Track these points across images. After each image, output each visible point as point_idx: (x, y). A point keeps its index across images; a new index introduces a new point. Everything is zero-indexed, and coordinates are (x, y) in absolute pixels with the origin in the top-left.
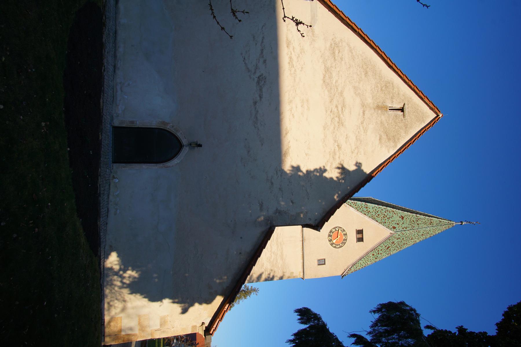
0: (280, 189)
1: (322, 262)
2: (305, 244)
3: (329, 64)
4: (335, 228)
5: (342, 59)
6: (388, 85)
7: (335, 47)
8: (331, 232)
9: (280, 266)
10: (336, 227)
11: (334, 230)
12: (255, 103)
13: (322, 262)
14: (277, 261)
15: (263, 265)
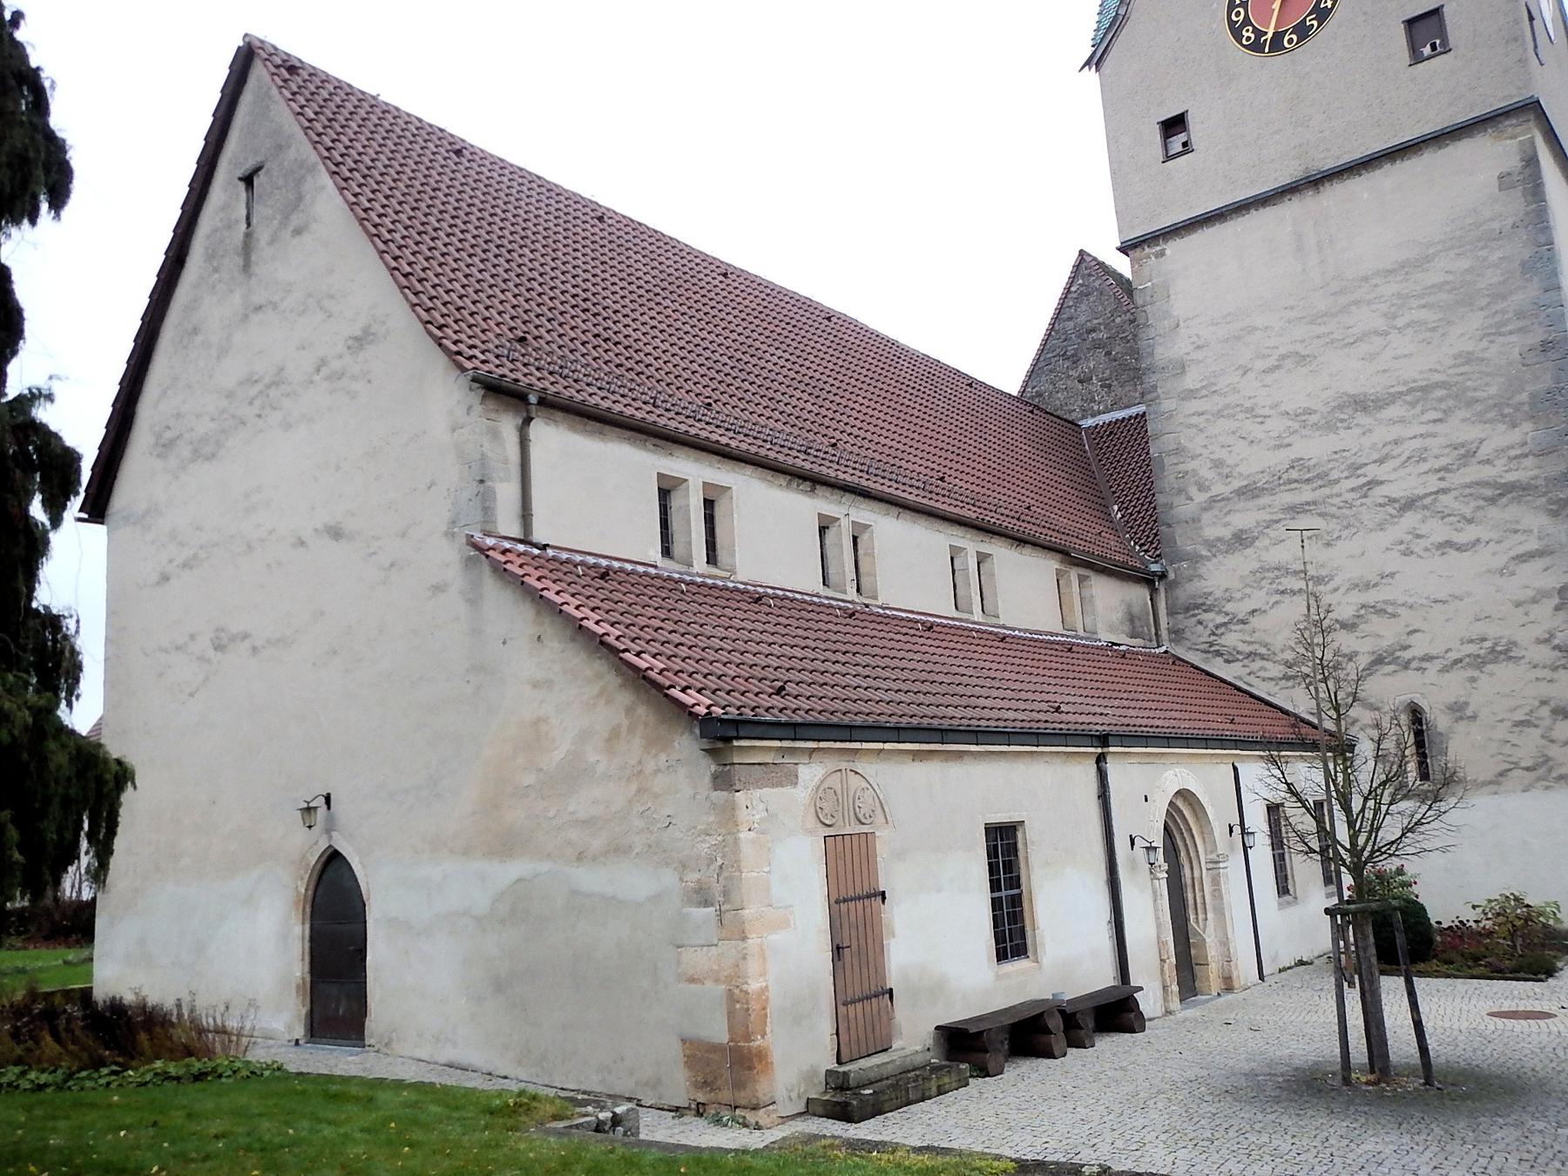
0: (403, 535)
1: (1426, 31)
2: (1329, 164)
3: (186, 452)
4: (1237, 35)
5: (178, 416)
6: (210, 256)
7: (165, 447)
8: (1256, 47)
9: (1465, 264)
10: (1231, 23)
11: (1248, 33)
12: (255, 649)
13: (1426, 31)
14: (1439, 287)
15: (1468, 358)
